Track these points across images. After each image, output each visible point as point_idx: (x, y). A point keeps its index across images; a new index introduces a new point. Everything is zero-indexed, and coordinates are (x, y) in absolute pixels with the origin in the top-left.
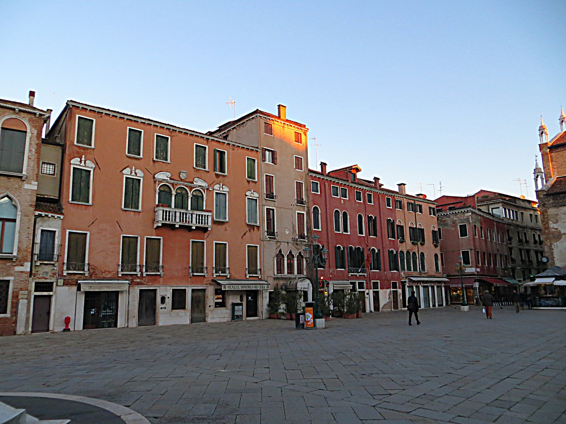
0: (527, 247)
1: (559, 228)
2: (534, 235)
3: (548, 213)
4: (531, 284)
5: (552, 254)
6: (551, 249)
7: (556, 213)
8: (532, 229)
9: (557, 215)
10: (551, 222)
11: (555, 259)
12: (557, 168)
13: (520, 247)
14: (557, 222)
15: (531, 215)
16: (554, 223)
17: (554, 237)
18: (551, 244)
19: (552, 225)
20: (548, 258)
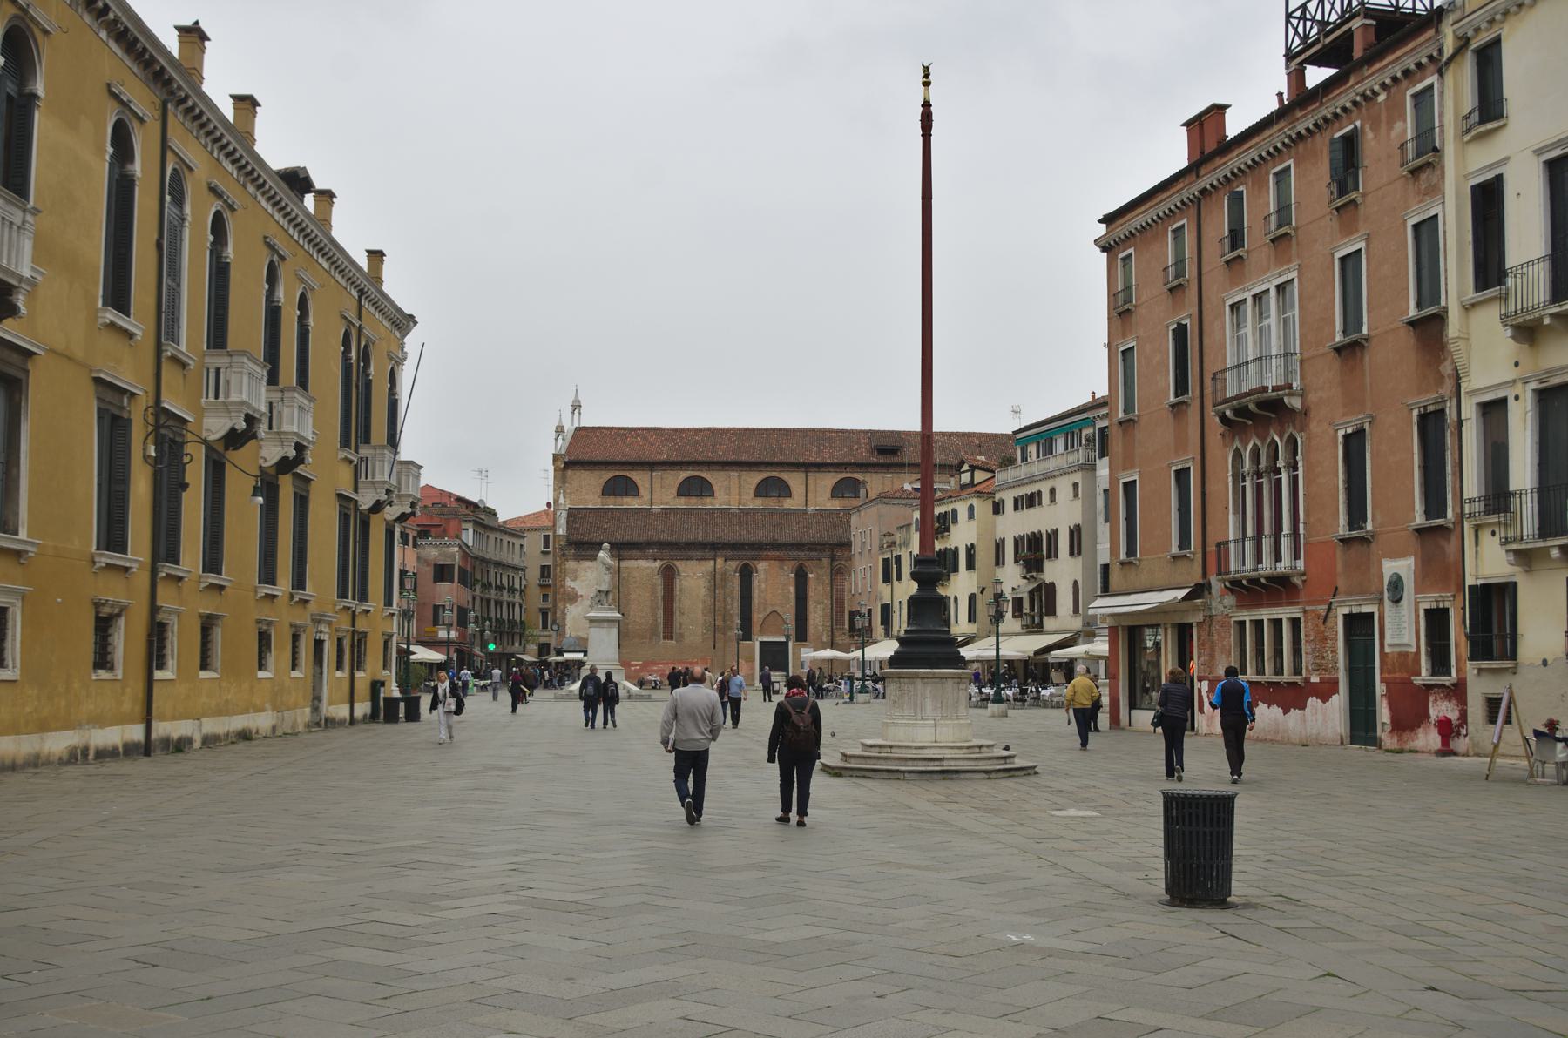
0: (487, 596)
1: (577, 588)
2: (496, 573)
3: (567, 566)
4: (559, 658)
5: (564, 619)
6: (564, 614)
7: (576, 566)
8: (497, 564)
9: (577, 570)
10: (568, 579)
11: (567, 627)
12: (571, 494)
13: (482, 595)
14: (574, 579)
15: (496, 539)
16: (572, 580)
17: (570, 599)
18: (565, 607)
19: (569, 583)
20: (558, 626)
